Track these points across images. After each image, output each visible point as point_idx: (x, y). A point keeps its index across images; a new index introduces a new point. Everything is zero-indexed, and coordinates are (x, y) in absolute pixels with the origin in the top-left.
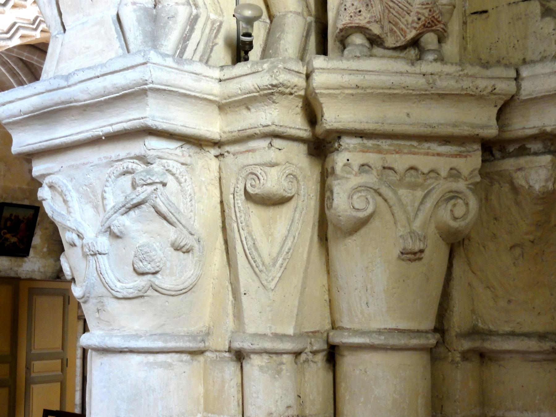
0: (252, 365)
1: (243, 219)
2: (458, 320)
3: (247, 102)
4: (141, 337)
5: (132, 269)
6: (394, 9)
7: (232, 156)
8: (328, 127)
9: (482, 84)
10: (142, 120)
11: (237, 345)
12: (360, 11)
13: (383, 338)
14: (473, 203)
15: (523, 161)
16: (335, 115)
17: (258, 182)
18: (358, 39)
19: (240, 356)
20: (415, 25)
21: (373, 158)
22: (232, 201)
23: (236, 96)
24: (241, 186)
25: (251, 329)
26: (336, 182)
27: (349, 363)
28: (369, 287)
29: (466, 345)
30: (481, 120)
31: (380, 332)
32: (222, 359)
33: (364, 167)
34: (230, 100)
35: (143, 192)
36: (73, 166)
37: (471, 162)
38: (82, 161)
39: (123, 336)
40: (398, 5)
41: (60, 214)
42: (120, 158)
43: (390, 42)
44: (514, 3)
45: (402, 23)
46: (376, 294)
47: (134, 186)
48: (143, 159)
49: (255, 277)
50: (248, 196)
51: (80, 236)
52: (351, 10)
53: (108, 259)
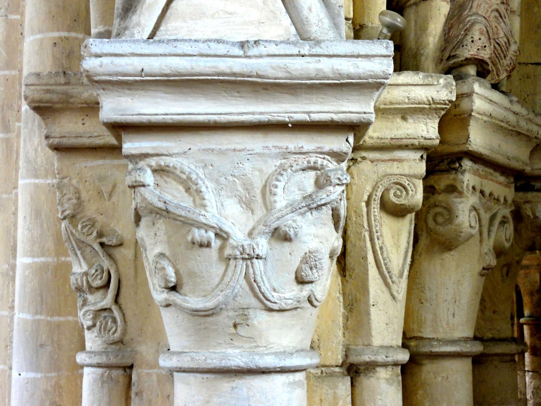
0: (378, 378)
1: (378, 228)
4: (292, 354)
5: (293, 276)
6: (497, 51)
7: (369, 163)
8: (470, 149)
10: (365, 116)
12: (485, 47)
13: (468, 346)
17: (405, 193)
18: (472, 70)
20: (507, 68)
22: (365, 209)
23: (399, 104)
24: (379, 194)
25: (377, 341)
26: (458, 200)
28: (458, 298)
32: (332, 375)
34: (391, 106)
36: (213, 150)
38: (232, 147)
39: (276, 354)
40: (501, 48)
41: (178, 206)
42: (304, 150)
44: (524, 63)
45: (500, 64)
47: (319, 185)
49: (384, 289)
51: (222, 235)
52: (479, 44)
53: (265, 265)
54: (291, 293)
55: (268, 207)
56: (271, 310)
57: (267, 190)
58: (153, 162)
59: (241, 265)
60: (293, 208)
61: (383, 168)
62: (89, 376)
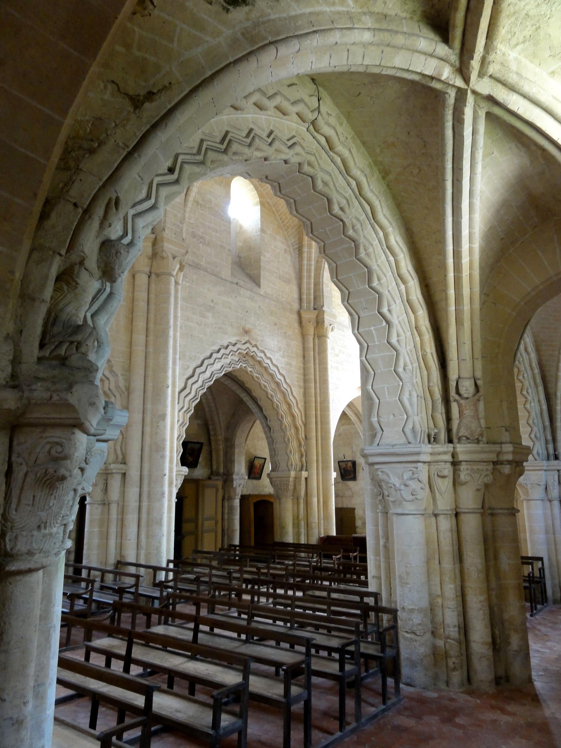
2: (487, 505)
3: (439, 454)
11: (436, 512)
14: (492, 477)
15: (502, 466)
16: (461, 457)
18: (464, 438)
19: (436, 515)
21: (469, 467)
25: (440, 508)
27: (463, 517)
29: (489, 511)
30: (493, 457)
31: (471, 509)
33: (467, 469)
35: (416, 476)
37: (491, 467)
43: (471, 439)
46: (469, 499)
47: (413, 474)
48: (417, 468)
50: (438, 475)
51: (394, 485)
54: (411, 497)
55: (403, 479)
57: (402, 476)
59: (399, 492)
60: (407, 479)
61: (436, 467)
62: (380, 514)
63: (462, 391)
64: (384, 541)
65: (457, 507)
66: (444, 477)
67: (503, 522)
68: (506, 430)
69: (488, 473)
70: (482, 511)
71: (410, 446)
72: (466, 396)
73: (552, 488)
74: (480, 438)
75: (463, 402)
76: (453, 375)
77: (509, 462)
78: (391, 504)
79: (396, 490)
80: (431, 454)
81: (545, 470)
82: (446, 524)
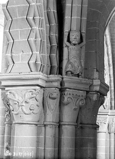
9: (88, 82)
11: (45, 123)
18: (70, 73)
19: (45, 126)
29: (81, 125)
37: (84, 94)
46: (68, 116)
47: (32, 94)
50: (49, 97)
56: (26, 114)
58: (9, 91)
63: (72, 38)
64: (7, 144)
65: (60, 121)
66: (54, 99)
67: (87, 130)
68: (97, 71)
69: (83, 98)
70: (76, 124)
71: (31, 73)
72: (74, 42)
73: (111, 126)
74: (80, 74)
75: (71, 47)
76: (66, 30)
77: (97, 92)
78: (14, 115)
79: (19, 106)
80: (46, 82)
81: (109, 115)
82: (50, 132)
